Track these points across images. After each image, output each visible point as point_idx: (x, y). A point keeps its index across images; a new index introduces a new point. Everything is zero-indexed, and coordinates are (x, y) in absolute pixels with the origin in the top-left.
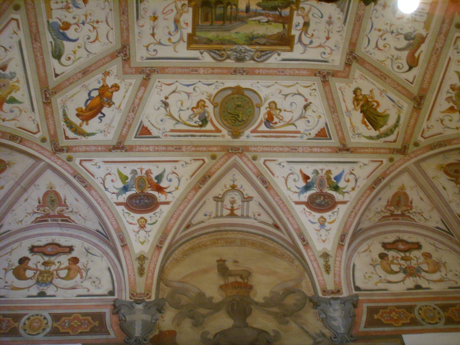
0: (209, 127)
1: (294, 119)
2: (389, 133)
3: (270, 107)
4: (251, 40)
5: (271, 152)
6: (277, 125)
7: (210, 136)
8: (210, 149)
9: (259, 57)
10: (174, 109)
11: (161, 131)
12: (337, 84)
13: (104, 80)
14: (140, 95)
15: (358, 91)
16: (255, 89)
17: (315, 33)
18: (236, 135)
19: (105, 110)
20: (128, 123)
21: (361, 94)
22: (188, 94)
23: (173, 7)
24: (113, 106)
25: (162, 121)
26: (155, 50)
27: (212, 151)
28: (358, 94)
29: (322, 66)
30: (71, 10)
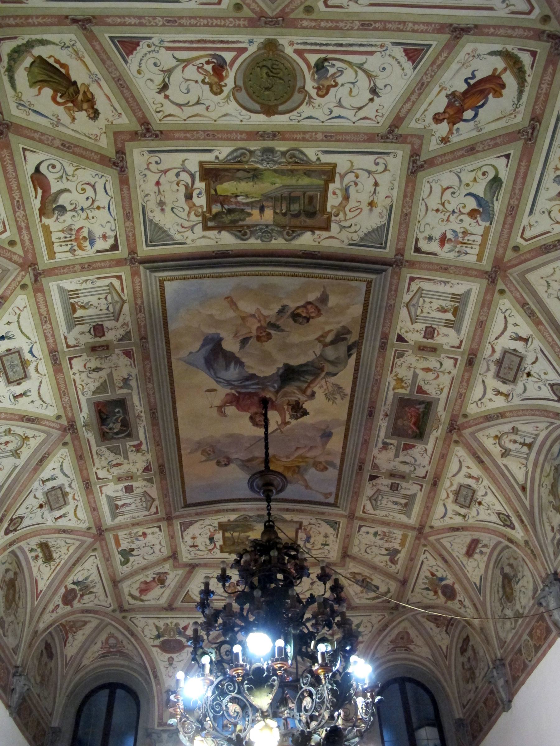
0: (313, 59)
1: (180, 68)
2: (16, 55)
3: (221, 86)
4: (255, 175)
5: (211, 18)
6: (207, 59)
7: (312, 44)
8: (313, 24)
9: (243, 154)
10: (364, 83)
11: (388, 52)
12: (126, 121)
13: (450, 132)
14: (408, 106)
15: (92, 116)
16: (244, 112)
17: (175, 187)
18: (271, 45)
19: (462, 87)
20: (435, 67)
21: (86, 110)
22: (340, 105)
23: (350, 215)
24: (449, 93)
25: (384, 69)
26: (377, 164)
27: (312, 20)
28: (91, 111)
29: (155, 145)
30: (462, 230)
